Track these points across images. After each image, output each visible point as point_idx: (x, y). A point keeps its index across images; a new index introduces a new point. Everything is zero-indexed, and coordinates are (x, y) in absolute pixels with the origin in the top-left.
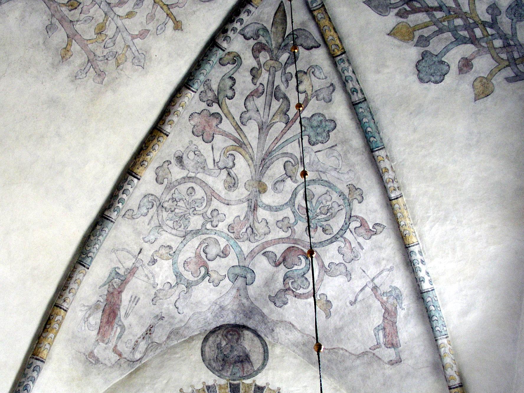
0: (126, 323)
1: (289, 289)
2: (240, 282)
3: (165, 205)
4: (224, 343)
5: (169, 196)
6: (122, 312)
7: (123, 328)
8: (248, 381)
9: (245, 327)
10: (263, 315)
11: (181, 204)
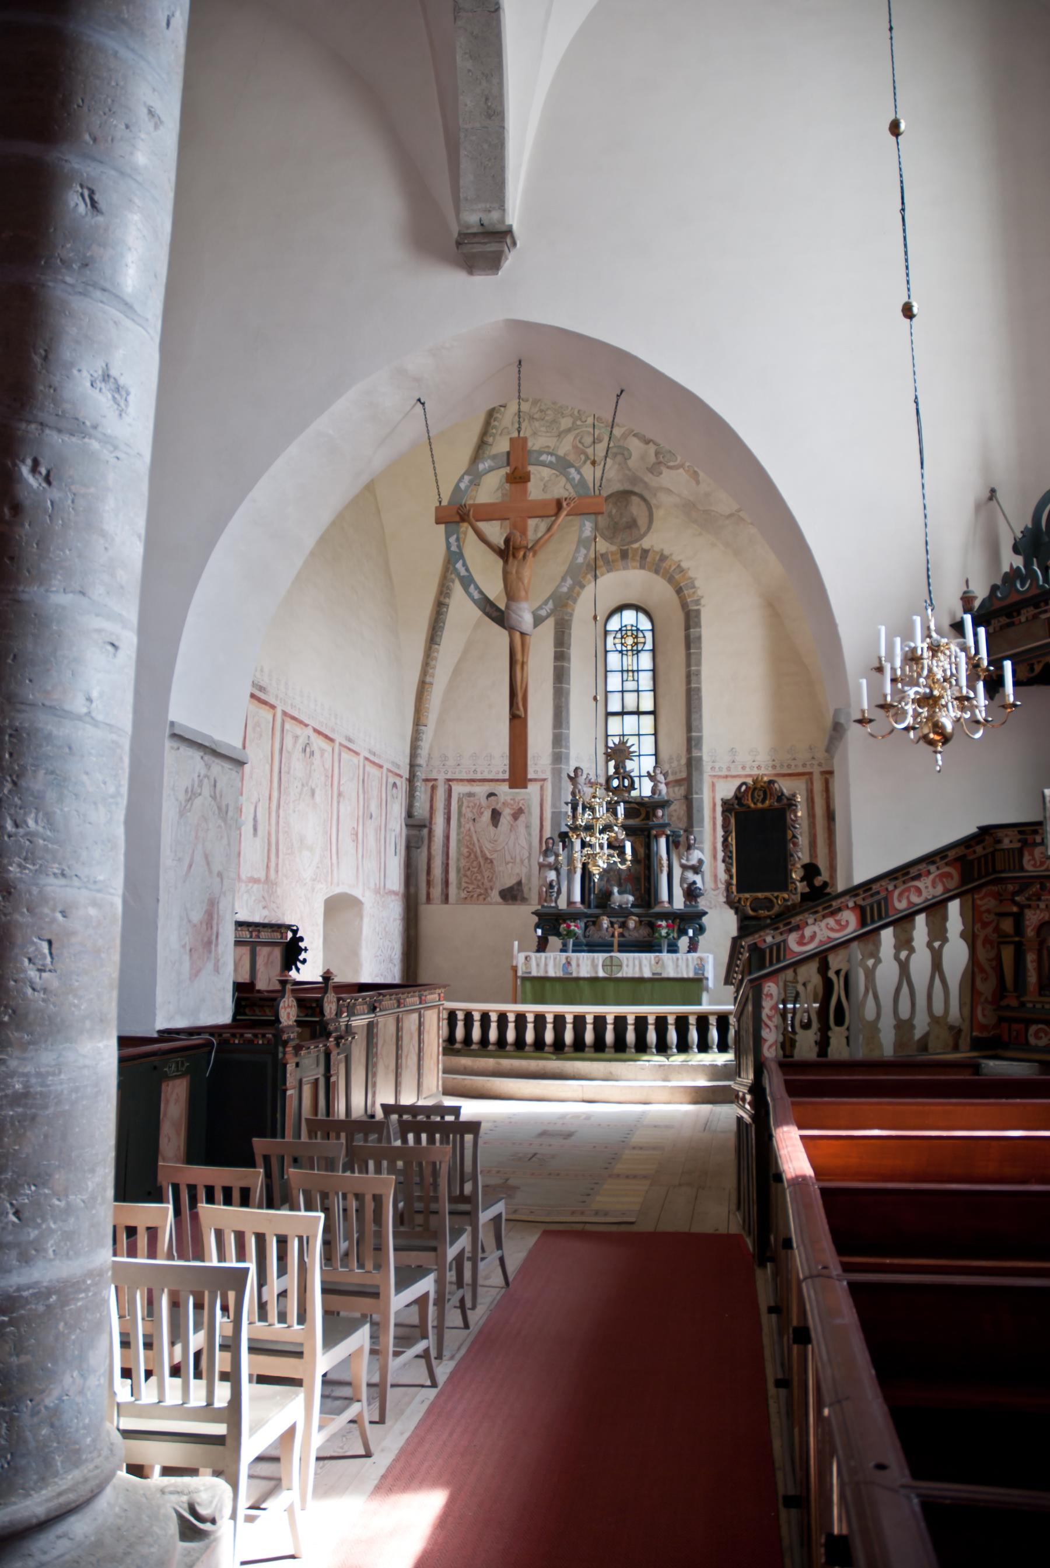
1: (660, 463)
2: (619, 458)
3: (536, 416)
4: (614, 511)
5: (537, 409)
8: (636, 546)
9: (632, 493)
10: (645, 483)
11: (549, 412)
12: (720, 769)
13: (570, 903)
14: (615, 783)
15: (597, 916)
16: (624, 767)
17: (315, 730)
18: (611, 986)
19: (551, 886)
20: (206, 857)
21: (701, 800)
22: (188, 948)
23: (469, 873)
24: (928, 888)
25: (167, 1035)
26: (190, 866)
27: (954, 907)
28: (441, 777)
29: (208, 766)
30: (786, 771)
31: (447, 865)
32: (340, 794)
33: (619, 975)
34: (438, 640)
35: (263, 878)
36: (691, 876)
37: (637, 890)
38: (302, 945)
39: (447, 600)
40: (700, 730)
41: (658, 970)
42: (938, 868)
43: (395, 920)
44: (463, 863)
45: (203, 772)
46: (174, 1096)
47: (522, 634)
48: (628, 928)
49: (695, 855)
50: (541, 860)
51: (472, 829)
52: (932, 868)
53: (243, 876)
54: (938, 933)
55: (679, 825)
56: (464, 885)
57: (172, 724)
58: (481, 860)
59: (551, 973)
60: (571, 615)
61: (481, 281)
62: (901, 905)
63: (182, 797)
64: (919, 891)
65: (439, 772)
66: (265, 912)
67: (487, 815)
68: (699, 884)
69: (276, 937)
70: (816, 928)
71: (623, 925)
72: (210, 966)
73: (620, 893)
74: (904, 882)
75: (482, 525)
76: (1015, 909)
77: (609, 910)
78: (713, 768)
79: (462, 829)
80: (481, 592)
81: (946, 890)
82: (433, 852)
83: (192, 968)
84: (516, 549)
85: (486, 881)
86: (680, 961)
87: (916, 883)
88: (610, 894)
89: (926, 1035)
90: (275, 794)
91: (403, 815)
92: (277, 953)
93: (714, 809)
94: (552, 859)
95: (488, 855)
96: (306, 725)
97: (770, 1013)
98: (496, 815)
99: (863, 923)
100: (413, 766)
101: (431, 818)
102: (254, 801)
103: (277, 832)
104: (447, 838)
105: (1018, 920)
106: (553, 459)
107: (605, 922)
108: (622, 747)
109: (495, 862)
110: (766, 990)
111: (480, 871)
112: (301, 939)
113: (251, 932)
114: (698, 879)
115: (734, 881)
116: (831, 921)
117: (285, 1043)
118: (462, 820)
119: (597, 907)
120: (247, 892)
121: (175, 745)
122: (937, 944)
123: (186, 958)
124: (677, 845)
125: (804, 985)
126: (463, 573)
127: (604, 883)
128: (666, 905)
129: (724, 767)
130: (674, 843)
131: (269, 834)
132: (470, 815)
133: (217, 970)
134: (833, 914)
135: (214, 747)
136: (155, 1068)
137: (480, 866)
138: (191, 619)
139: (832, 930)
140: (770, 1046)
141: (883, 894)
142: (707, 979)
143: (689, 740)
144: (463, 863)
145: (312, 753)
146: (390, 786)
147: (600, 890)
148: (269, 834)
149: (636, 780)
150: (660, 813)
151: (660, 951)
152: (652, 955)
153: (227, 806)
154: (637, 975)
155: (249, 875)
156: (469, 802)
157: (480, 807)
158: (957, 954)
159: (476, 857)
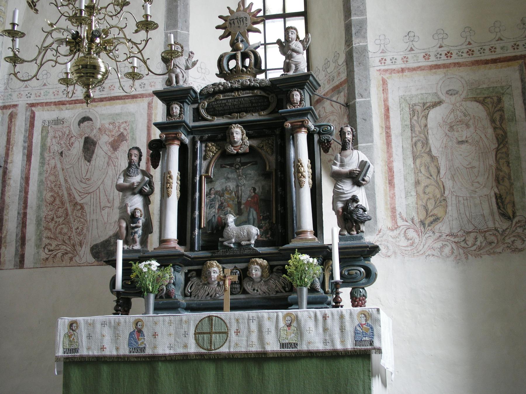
12: (393, 60)
13: (163, 241)
14: (232, 64)
15: (202, 262)
16: (245, 41)
18: (210, 369)
19: (133, 218)
21: (368, 105)
23: (52, 225)
28: (22, 103)
30: (489, 56)
31: (25, 214)
33: (224, 349)
36: (348, 189)
37: (264, 219)
40: (363, 12)
41: (291, 338)
44: (45, 211)
48: (251, 279)
49: (353, 159)
50: (121, 181)
51: (59, 166)
55: (331, 115)
56: (45, 241)
58: (68, 205)
59: (110, 351)
65: (20, 95)
67: (79, 145)
68: (363, 201)
71: (245, 274)
73: (238, 223)
77: (221, 252)
78: (382, 61)
79: (46, 166)
85: (74, 233)
86: (329, 321)
88: (224, 225)
93: (387, 117)
94: (136, 179)
95: (78, 199)
98: (89, 146)
104: (27, 179)
107: (215, 270)
108: (242, 15)
109: (86, 207)
111: (66, 222)
114: (360, 193)
118: (46, 155)
119: (203, 248)
124: (326, 146)
127: (214, 210)
128: (310, 236)
129: (399, 58)
130: (320, 143)
132: (56, 148)
137: (67, 215)
142: (379, 351)
143: (348, 28)
144: (45, 211)
147: (209, 222)
149: (260, 51)
150: (297, 96)
151: (296, 304)
152: (281, 313)
154: (255, 348)
156: (55, 131)
157: (70, 136)
159: (63, 203)
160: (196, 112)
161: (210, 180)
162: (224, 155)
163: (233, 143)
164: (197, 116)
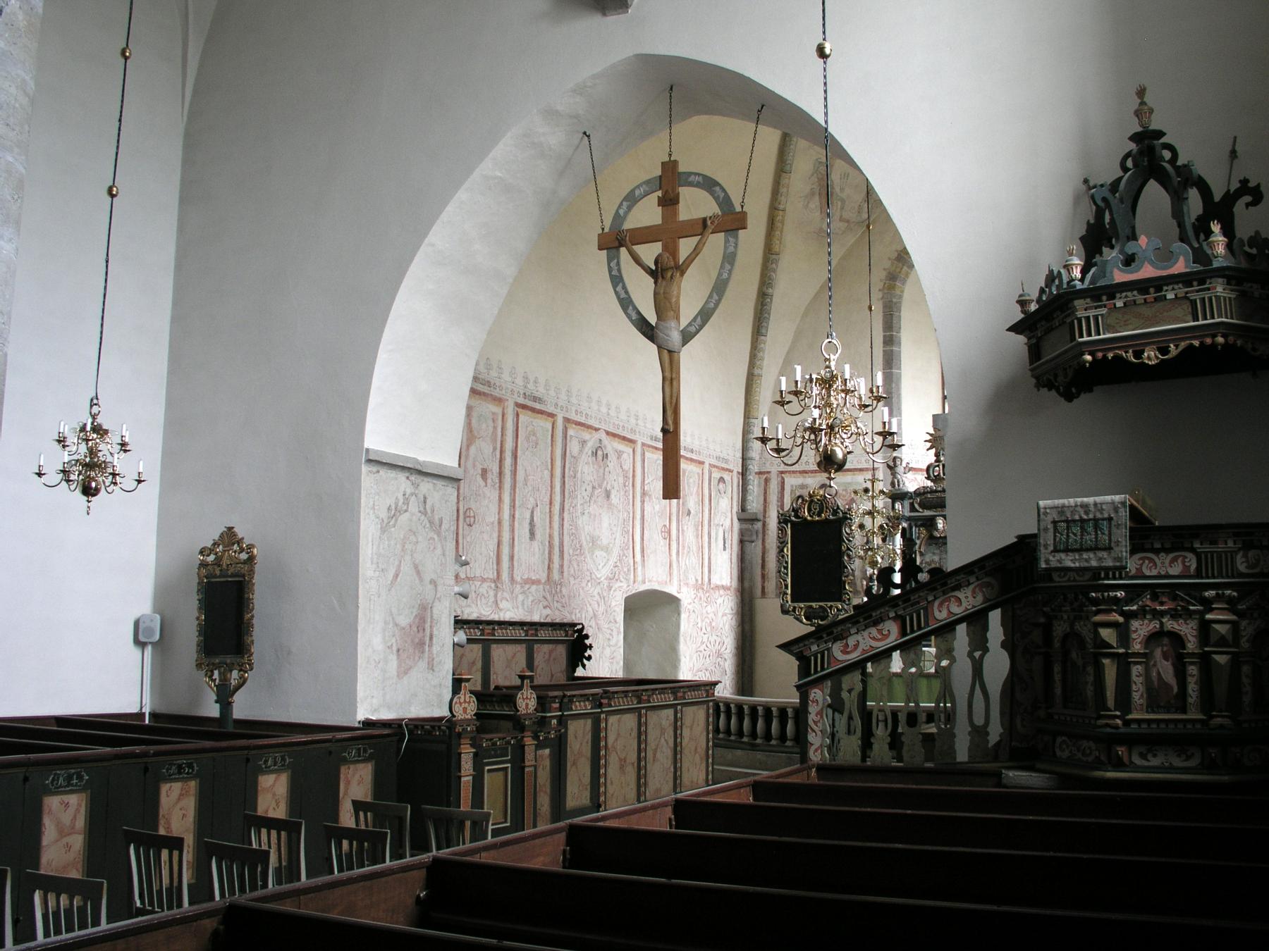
0: (844, 195)
6: (837, 189)
7: (843, 201)
17: (608, 433)
20: (416, 567)
22: (395, 649)
24: (967, 600)
25: (368, 724)
26: (396, 576)
27: (995, 617)
29: (416, 486)
32: (644, 494)
34: (764, 331)
35: (543, 576)
38: (587, 642)
39: (770, 291)
42: (978, 579)
43: (724, 615)
45: (408, 491)
46: (357, 777)
47: (670, 351)
52: (972, 579)
53: (518, 579)
54: (979, 642)
57: (367, 450)
60: (901, 297)
61: (613, 20)
62: (941, 614)
63: (384, 514)
64: (959, 600)
66: (548, 611)
69: (560, 635)
70: (859, 637)
72: (422, 664)
74: (944, 593)
75: (639, 249)
76: (1042, 620)
80: (639, 313)
81: (986, 600)
82: (767, 546)
83: (399, 666)
84: (664, 270)
87: (957, 593)
89: (998, 744)
90: (557, 498)
91: (735, 509)
92: (561, 651)
96: (597, 430)
97: (816, 719)
99: (903, 633)
100: (745, 459)
101: (765, 511)
102: (530, 506)
103: (561, 534)
105: (1047, 629)
106: (700, 179)
110: (812, 696)
112: (587, 637)
113: (526, 631)
115: (789, 591)
116: (874, 631)
117: (459, 735)
120: (524, 592)
121: (374, 469)
122: (977, 654)
123: (393, 658)
125: (850, 691)
126: (623, 295)
131: (551, 536)
133: (431, 667)
134: (875, 623)
135: (419, 467)
136: (330, 753)
138: (382, 356)
139: (874, 639)
140: (816, 750)
141: (923, 604)
145: (606, 456)
146: (714, 482)
148: (551, 536)
153: (441, 520)
155: (526, 577)
158: (998, 664)
160: (912, 505)
161: (922, 554)
162: (931, 537)
163: (937, 530)
164: (913, 509)
